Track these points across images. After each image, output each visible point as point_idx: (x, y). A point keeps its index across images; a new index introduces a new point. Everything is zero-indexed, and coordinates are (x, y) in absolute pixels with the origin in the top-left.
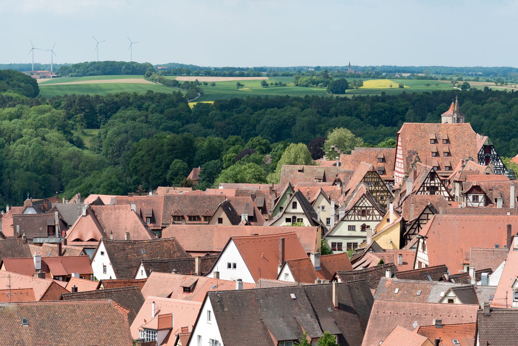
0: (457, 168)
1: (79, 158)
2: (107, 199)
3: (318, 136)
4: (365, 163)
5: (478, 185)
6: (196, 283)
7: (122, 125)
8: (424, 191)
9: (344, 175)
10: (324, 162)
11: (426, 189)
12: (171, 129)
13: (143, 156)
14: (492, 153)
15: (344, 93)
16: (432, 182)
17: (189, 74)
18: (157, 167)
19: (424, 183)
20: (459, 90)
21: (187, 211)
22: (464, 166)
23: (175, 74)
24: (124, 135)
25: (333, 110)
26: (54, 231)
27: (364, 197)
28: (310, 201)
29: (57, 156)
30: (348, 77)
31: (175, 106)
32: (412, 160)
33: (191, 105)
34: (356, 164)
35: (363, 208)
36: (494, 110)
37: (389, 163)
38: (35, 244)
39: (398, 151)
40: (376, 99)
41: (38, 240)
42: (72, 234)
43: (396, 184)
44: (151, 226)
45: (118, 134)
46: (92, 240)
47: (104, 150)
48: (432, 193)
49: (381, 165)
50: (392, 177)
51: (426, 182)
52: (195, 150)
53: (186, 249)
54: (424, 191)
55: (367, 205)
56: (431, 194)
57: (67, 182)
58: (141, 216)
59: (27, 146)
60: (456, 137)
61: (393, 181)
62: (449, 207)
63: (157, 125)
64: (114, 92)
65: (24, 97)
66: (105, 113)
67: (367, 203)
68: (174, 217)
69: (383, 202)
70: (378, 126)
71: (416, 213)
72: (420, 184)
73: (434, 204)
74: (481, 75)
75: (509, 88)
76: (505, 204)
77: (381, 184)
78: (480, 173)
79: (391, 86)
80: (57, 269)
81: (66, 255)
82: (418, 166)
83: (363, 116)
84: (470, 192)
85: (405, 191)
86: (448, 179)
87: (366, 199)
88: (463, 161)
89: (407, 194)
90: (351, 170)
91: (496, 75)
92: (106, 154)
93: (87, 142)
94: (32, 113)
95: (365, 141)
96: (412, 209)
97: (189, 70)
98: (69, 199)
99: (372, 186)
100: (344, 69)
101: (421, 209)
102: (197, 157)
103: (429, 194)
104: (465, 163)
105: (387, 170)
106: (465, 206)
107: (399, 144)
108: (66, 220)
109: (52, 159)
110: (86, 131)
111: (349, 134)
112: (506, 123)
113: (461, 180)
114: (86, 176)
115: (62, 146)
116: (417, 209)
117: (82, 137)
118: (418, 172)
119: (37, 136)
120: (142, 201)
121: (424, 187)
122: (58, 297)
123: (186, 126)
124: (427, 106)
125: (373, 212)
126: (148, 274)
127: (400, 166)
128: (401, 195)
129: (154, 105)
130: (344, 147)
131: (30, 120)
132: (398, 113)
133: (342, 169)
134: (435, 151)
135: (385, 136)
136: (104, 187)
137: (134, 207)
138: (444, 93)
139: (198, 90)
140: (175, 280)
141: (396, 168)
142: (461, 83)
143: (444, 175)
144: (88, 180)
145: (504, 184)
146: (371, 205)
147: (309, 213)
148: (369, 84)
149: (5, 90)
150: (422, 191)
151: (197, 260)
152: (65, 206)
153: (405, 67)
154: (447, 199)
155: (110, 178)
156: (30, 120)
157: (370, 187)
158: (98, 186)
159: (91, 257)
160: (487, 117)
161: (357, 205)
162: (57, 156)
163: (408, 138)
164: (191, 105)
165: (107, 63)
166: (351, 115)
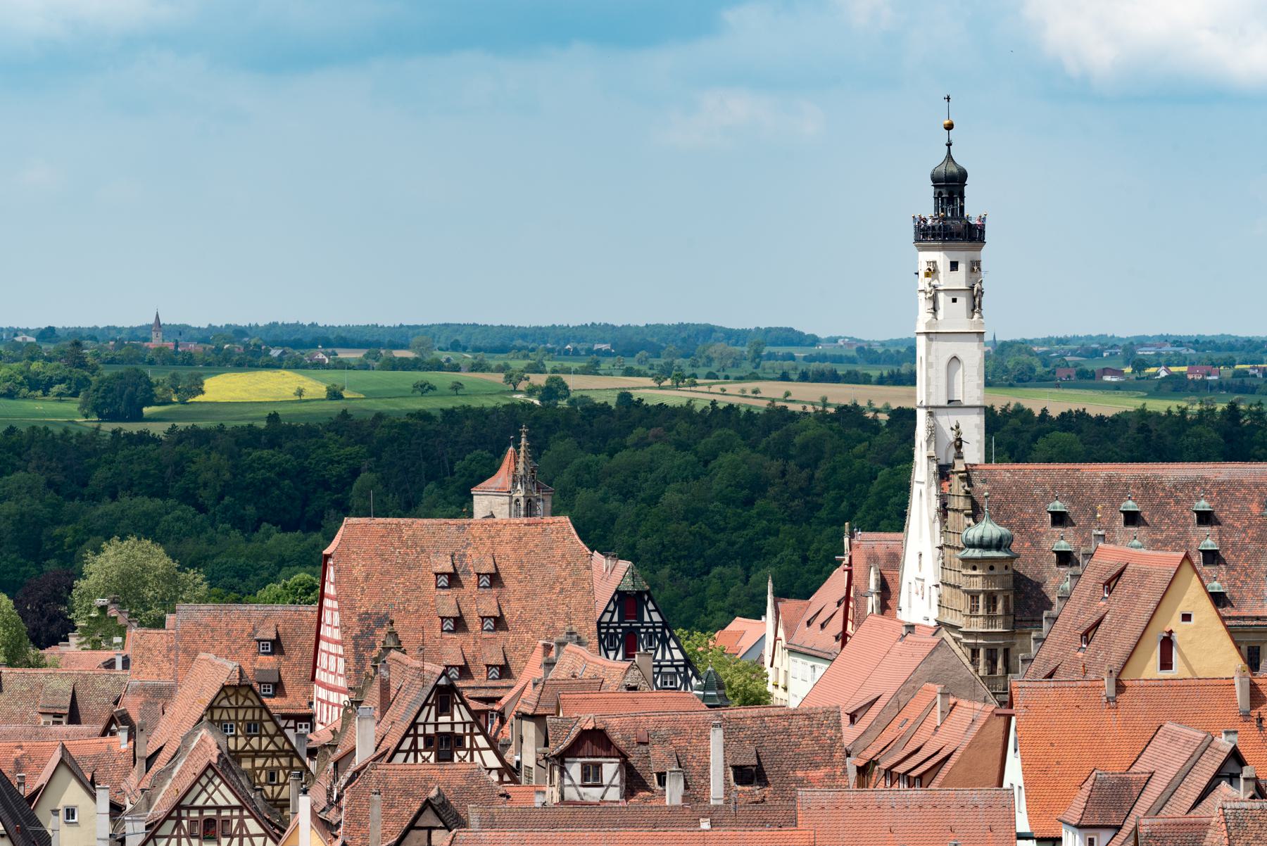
0: (530, 671)
3: (52, 565)
4: (212, 656)
5: (600, 726)
8: (416, 751)
9: (140, 700)
10: (74, 656)
11: (421, 745)
14: (647, 618)
15: (139, 417)
16: (441, 719)
19: (414, 725)
20: (532, 405)
22: (549, 665)
25: (100, 475)
27: (210, 773)
28: (25, 791)
30: (151, 362)
32: (373, 646)
34: (185, 660)
35: (207, 813)
36: (651, 471)
37: (296, 655)
39: (327, 616)
40: (248, 438)
43: (319, 727)
48: (444, 757)
49: (268, 662)
50: (305, 704)
51: (422, 719)
54: (416, 751)
55: (222, 802)
56: (438, 759)
60: (521, 567)
61: (309, 718)
62: (500, 806)
67: (222, 795)
69: (277, 789)
70: (256, 529)
71: (391, 825)
72: (403, 726)
73: (449, 795)
74: (607, 354)
75: (702, 395)
76: (694, 792)
77: (270, 728)
78: (605, 685)
79: (300, 392)
82: (394, 667)
83: (205, 495)
84: (572, 751)
85: (352, 752)
86: (497, 707)
87: (217, 781)
88: (548, 648)
89: (358, 761)
90: (166, 681)
91: (656, 352)
95: (213, 580)
96: (376, 811)
99: (236, 736)
100: (138, 335)
101: (406, 813)
103: (432, 759)
104: (553, 654)
105: (288, 680)
106: (556, 798)
107: (330, 589)
111: (157, 558)
112: (693, 515)
113: (540, 712)
116: (393, 811)
118: (394, 686)
121: (416, 736)
124: (423, 461)
125: (242, 824)
127: (333, 664)
128: (336, 764)
130: (141, 603)
132: (325, 484)
133: (133, 678)
134: (453, 612)
135: (282, 562)
138: (482, 413)
141: (320, 675)
142: (540, 380)
143: (482, 694)
145: (687, 722)
146: (235, 802)
147: (22, 831)
148: (223, 388)
150: (408, 752)
153: (348, 329)
154: (495, 777)
157: (232, 741)
160: (626, 494)
161: (187, 802)
163: (359, 572)
166: (163, 495)
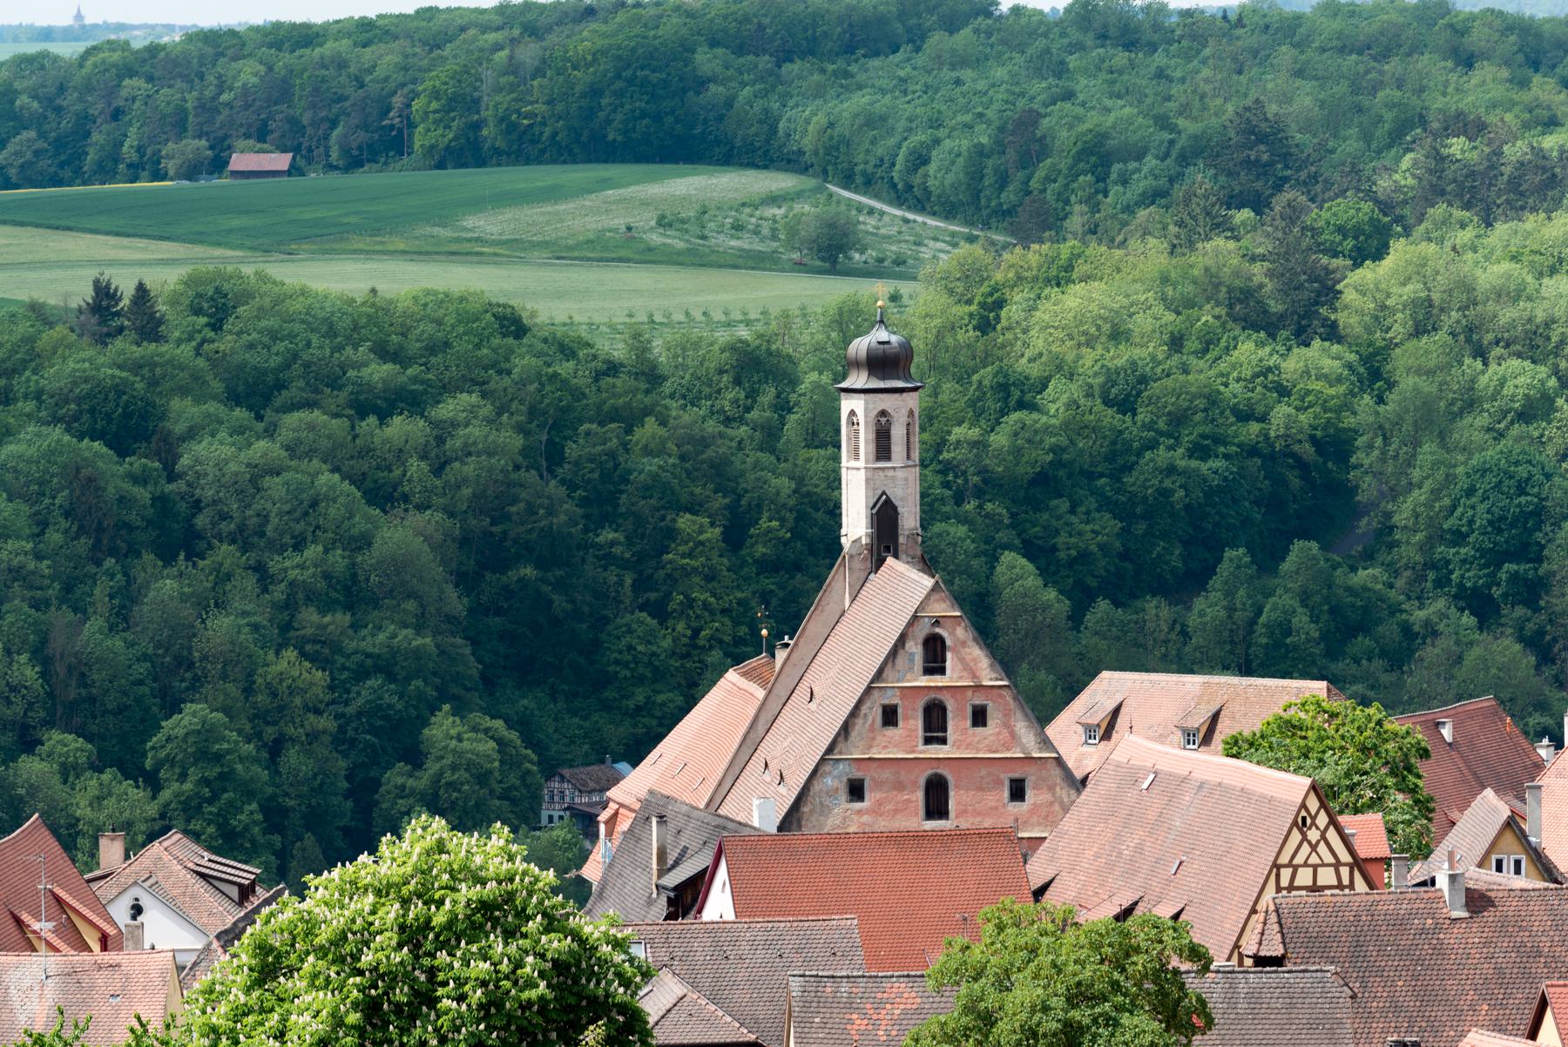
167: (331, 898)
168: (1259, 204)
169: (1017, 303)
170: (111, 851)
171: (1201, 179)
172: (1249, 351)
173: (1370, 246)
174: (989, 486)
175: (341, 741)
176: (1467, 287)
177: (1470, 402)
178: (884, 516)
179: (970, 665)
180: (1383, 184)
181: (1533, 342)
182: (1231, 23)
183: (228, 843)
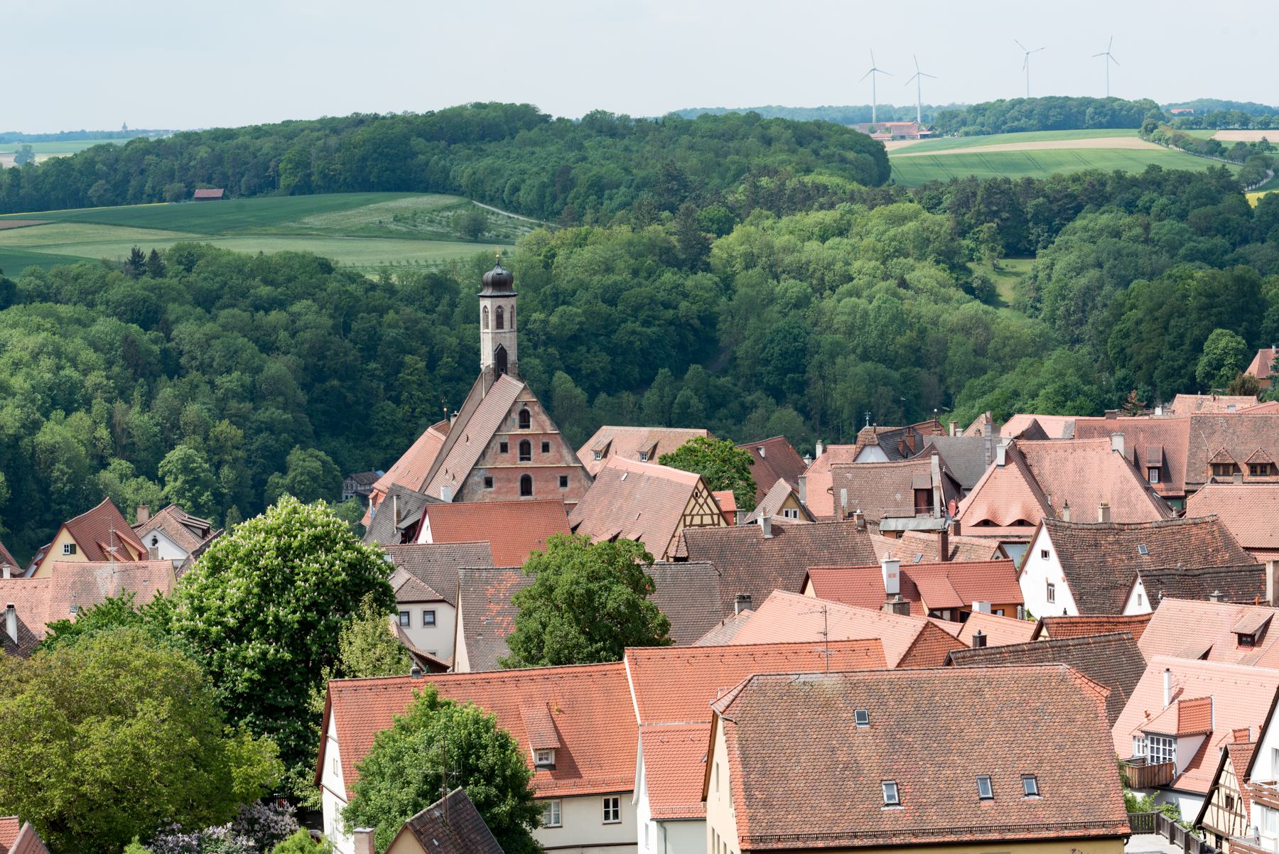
1: (987, 328)
2: (1055, 425)
6: (1267, 625)
7: (1088, 247)
12: (1206, 257)
13: (1138, 323)
17: (1245, 124)
18: (1173, 347)
21: (1245, 452)
23: (1213, 125)
24: (1093, 273)
26: (930, 502)
29: (935, 323)
31: (1214, 201)
33: (1253, 198)
38: (885, 533)
41: (893, 525)
42: (972, 509)
44: (1161, 488)
45: (1080, 270)
46: (1020, 523)
47: (1046, 308)
52: (1263, 305)
53: (1243, 542)
57: (960, 387)
58: (1136, 465)
59: (862, 302)
63: (1172, 248)
64: (1067, 171)
65: (855, 186)
66: (1049, 222)
68: (1215, 466)
80: (937, 592)
81: (959, 558)
92: (1052, 319)
93: (1006, 290)
94: (873, 222)
97: (1245, 117)
98: (966, 427)
102: (1267, 323)
108: (957, 476)
109: (922, 332)
110: (1003, 263)
114: (1004, 370)
115: (947, 300)
117: (993, 278)
119: (886, 277)
120: (1137, 430)
122: (941, 659)
123: (1240, 250)
126: (1154, 603)
129: (1163, 200)
131: (869, 241)
136: (1048, 398)
137: (1118, 442)
139: (1267, 163)
140: (1219, 617)
144: (1009, 381)
149: (808, 171)
151: (1270, 569)
152: (955, 437)
155: (1061, 375)
156: (869, 241)
158: (1034, 396)
159: (1017, 564)
162: (935, 323)
164: (1253, 198)
165: (1051, 102)
167: (244, 535)
168: (673, 209)
169: (562, 254)
170: (143, 514)
171: (646, 196)
172: (669, 277)
173: (724, 228)
174: (550, 340)
175: (249, 461)
176: (770, 246)
177: (771, 300)
178: (500, 355)
179: (541, 423)
180: (731, 198)
181: (800, 272)
182: (659, 124)
183: (197, 510)
